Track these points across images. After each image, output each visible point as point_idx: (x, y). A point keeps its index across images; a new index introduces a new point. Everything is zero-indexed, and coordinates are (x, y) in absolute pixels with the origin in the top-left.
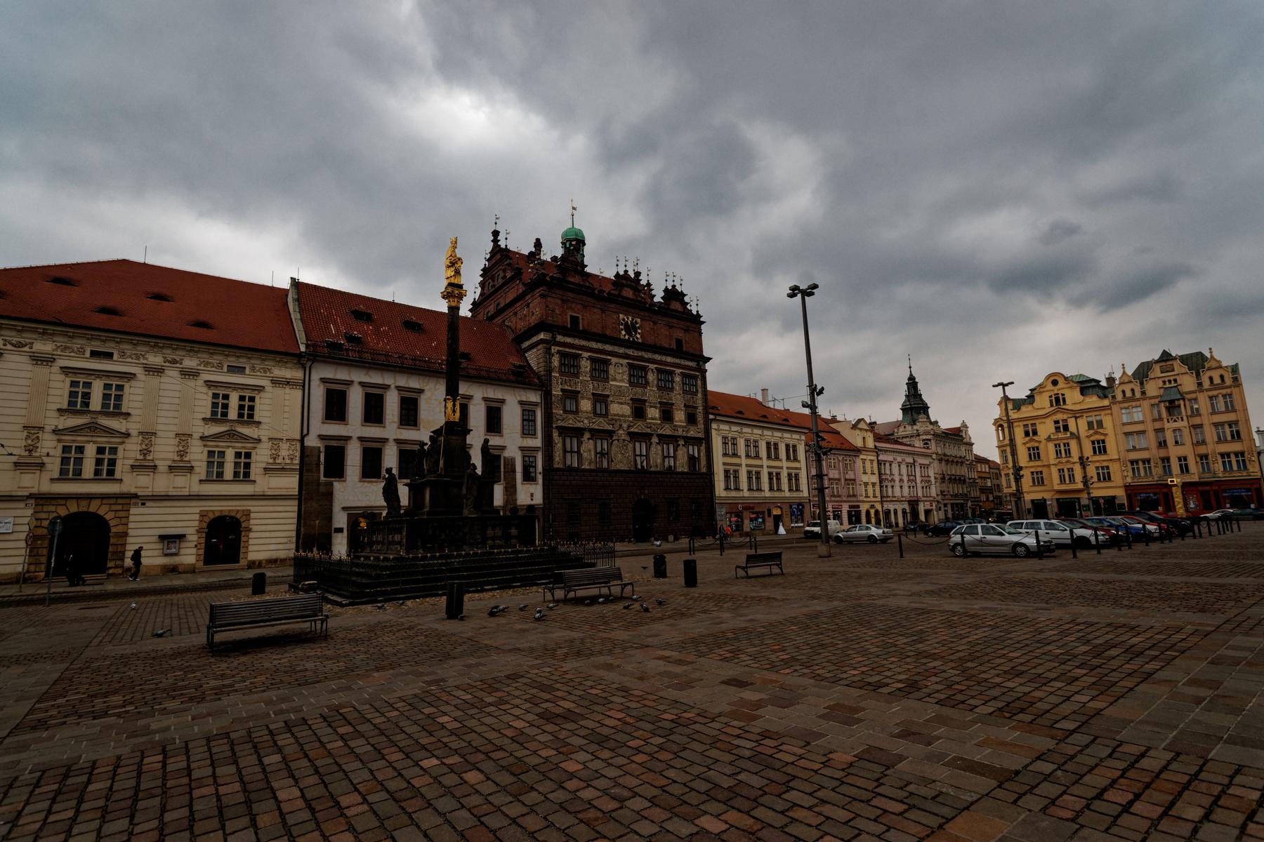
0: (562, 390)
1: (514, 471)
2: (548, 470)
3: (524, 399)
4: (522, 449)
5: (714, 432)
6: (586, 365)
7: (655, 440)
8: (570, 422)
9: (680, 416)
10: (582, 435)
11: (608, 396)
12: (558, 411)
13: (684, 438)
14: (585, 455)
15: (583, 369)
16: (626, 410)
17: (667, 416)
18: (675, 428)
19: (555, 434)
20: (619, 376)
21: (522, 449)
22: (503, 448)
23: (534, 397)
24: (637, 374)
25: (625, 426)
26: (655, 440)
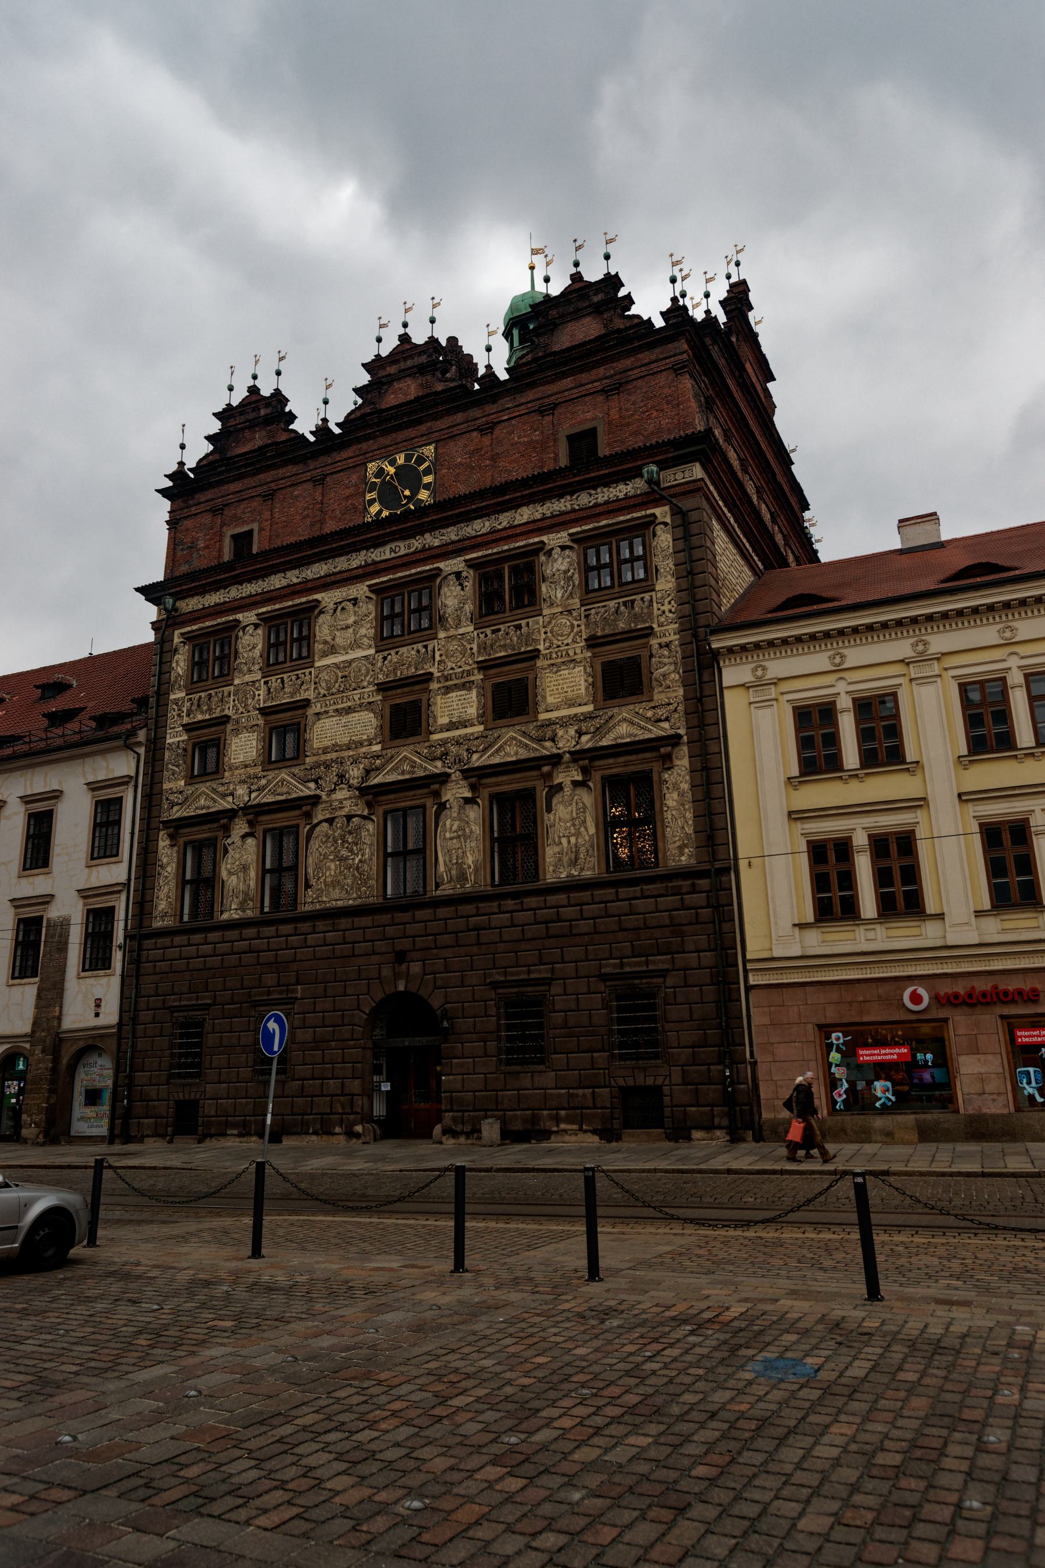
0: (188, 728)
1: (63, 947)
2: (140, 934)
3: (101, 776)
4: (84, 894)
5: (734, 705)
6: (252, 643)
7: (456, 791)
8: (206, 800)
9: (565, 687)
10: (227, 830)
11: (306, 703)
12: (174, 784)
13: (577, 755)
14: (232, 882)
15: (244, 655)
16: (365, 724)
17: (511, 697)
18: (547, 731)
19: (163, 843)
20: (347, 631)
21: (84, 894)
22: (47, 900)
23: (122, 765)
24: (404, 610)
25: (355, 773)
26: (456, 791)
